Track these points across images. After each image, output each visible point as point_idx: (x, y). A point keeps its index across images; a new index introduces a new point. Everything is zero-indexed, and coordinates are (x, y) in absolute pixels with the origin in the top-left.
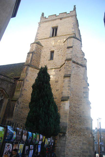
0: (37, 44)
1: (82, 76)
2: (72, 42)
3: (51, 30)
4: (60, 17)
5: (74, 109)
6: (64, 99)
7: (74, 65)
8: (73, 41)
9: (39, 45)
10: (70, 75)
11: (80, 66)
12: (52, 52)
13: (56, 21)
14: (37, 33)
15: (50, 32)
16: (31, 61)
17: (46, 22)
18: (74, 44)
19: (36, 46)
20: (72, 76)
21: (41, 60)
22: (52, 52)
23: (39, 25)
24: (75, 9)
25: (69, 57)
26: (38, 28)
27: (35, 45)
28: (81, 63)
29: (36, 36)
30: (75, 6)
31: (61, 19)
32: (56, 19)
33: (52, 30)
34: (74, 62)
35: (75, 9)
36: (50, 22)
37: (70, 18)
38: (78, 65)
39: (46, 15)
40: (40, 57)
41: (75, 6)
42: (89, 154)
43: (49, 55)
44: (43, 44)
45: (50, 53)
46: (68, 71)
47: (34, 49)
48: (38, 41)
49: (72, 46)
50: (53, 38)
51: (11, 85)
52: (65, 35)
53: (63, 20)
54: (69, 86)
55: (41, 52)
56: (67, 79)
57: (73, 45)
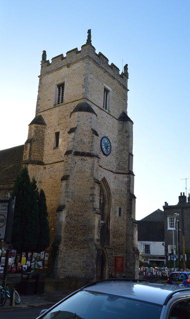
0: (36, 125)
1: (89, 171)
2: (76, 120)
3: (56, 91)
4: (68, 61)
5: (76, 218)
6: (60, 209)
7: (77, 158)
8: (78, 117)
9: (39, 126)
10: (69, 176)
11: (88, 158)
12: (57, 134)
13: (62, 71)
14: (39, 99)
15: (54, 96)
16: (30, 154)
17: (48, 73)
18: (79, 123)
19: (35, 129)
20: (71, 177)
21: (45, 149)
22: (57, 134)
23: (40, 80)
24: (89, 37)
25: (70, 148)
26: (39, 87)
27: (33, 126)
28: (90, 151)
29: (38, 105)
30: (89, 32)
31: (68, 66)
32: (61, 68)
33: (58, 90)
34: (77, 154)
35: (89, 37)
36: (55, 73)
37: (82, 62)
38: (84, 157)
39: (49, 58)
40: (43, 144)
41: (89, 32)
42: (92, 267)
43: (53, 140)
44: (46, 121)
45: (54, 135)
46: (67, 170)
47: (32, 135)
48: (40, 114)
49: (76, 128)
50: (57, 109)
51: (12, 191)
52: (73, 102)
53: (74, 67)
54: (66, 192)
55: (43, 135)
56: (64, 183)
57: (78, 125)
